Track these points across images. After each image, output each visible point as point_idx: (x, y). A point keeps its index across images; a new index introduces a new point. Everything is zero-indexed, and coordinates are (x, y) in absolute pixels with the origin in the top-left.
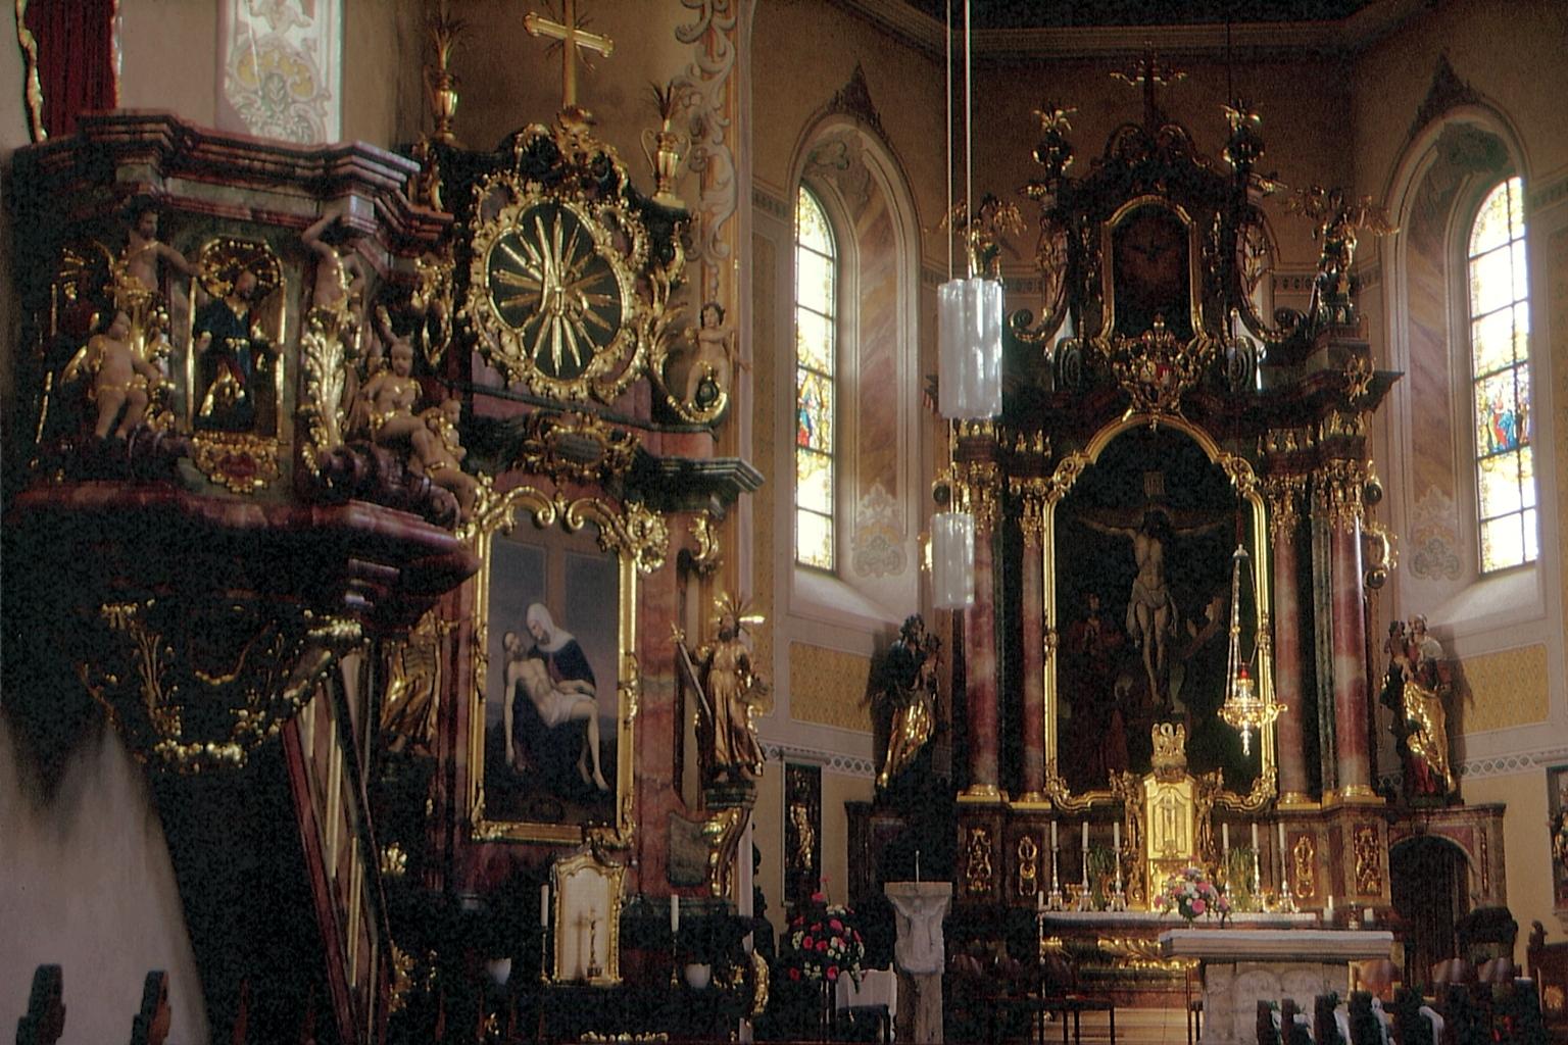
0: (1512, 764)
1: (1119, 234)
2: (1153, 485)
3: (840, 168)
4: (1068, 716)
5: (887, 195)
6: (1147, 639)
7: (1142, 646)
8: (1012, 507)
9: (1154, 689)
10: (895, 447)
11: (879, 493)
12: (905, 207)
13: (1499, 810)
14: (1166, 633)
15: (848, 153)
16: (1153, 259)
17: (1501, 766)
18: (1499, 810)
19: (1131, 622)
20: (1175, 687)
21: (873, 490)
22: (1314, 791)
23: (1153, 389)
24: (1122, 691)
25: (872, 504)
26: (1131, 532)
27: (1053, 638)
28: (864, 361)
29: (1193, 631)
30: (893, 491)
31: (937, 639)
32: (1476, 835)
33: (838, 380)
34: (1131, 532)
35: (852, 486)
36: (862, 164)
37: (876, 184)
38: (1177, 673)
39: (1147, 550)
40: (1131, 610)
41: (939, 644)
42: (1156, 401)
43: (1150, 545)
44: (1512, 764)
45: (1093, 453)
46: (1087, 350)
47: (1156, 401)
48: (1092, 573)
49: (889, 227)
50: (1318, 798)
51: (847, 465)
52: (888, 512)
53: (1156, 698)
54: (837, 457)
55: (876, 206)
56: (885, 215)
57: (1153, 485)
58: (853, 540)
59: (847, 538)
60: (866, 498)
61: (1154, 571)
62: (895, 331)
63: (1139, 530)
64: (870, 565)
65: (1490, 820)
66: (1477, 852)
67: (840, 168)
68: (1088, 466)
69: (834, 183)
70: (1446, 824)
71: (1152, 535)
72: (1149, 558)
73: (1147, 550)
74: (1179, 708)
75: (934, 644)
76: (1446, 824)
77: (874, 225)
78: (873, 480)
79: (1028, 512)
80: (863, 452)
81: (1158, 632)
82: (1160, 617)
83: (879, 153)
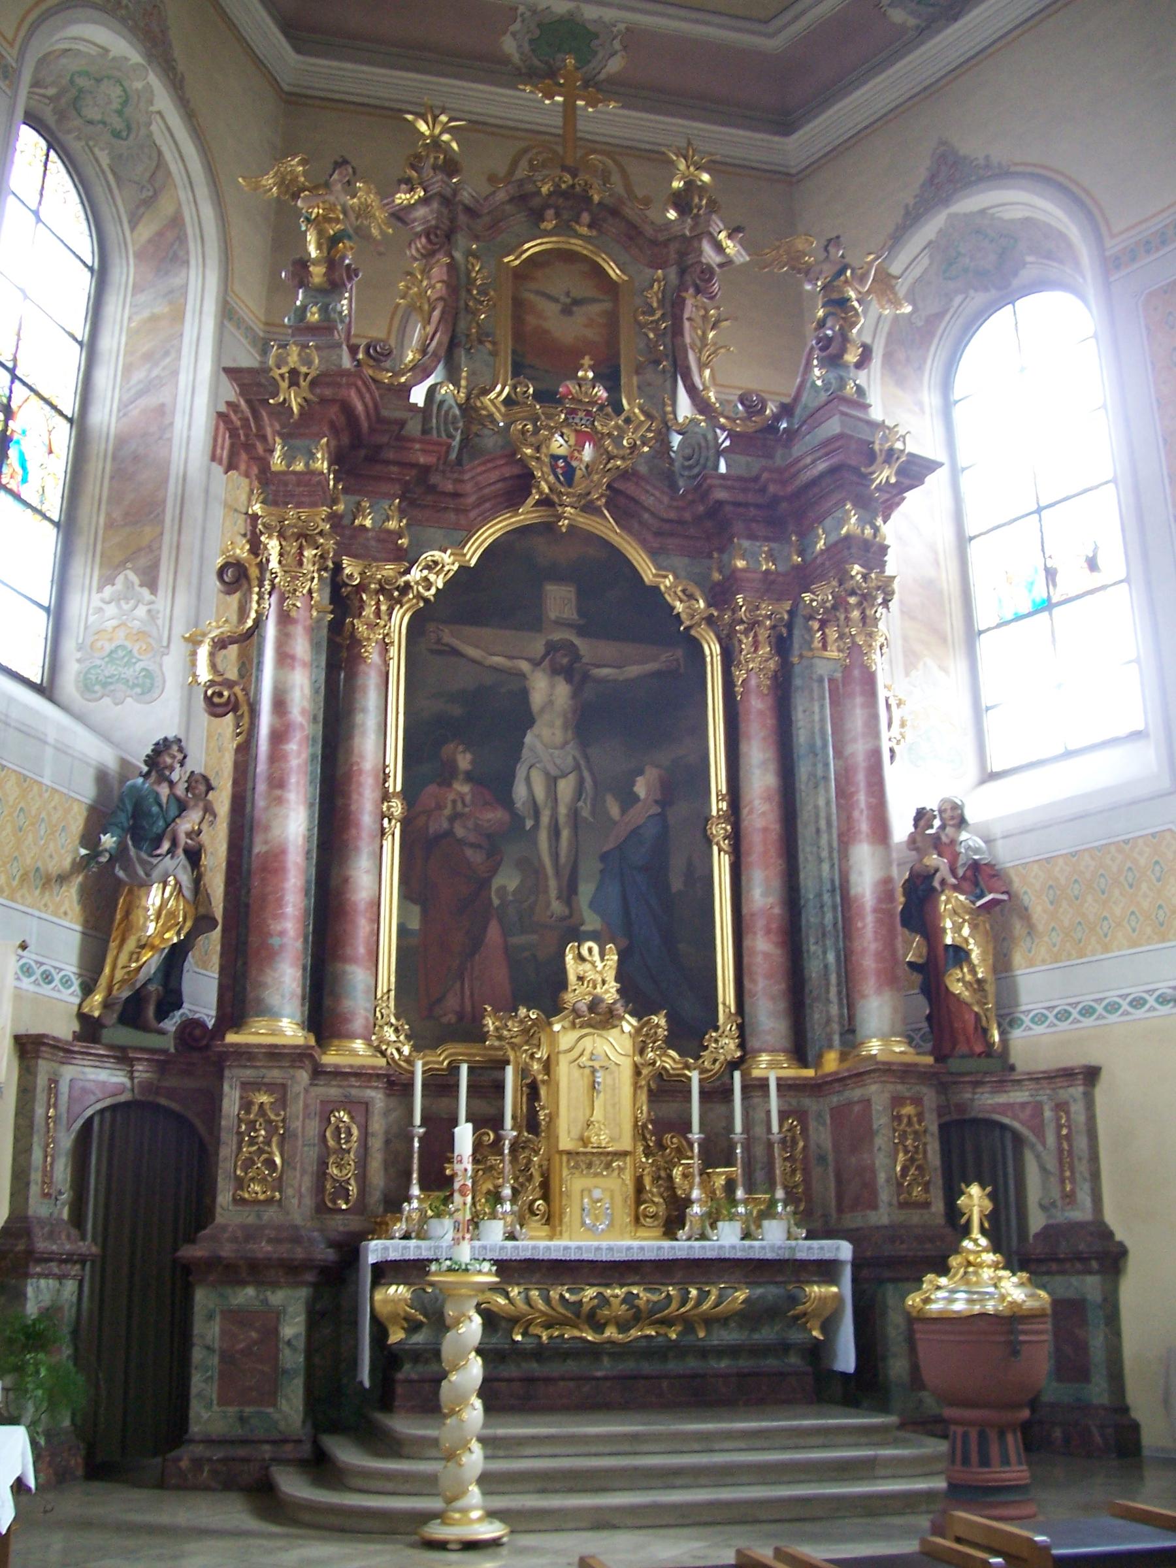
0: (1112, 1008)
1: (521, 275)
2: (559, 600)
3: (117, 135)
4: (415, 924)
5: (183, 195)
6: (545, 819)
7: (536, 826)
8: (343, 601)
9: (553, 893)
10: (162, 522)
11: (129, 585)
12: (208, 212)
13: (1091, 1074)
14: (574, 814)
15: (128, 110)
16: (567, 311)
17: (1088, 1011)
18: (1091, 1074)
19: (520, 792)
20: (586, 890)
21: (120, 580)
22: (800, 1052)
23: (568, 464)
24: (502, 890)
25: (116, 599)
26: (524, 666)
27: (397, 807)
28: (124, 406)
29: (614, 810)
30: (151, 584)
31: (206, 779)
32: (1048, 1114)
33: (79, 423)
34: (524, 666)
35: (83, 571)
36: (150, 135)
37: (169, 174)
38: (590, 868)
39: (548, 693)
40: (521, 772)
41: (210, 788)
42: (570, 485)
43: (552, 686)
44: (1112, 1008)
45: (473, 554)
46: (468, 409)
47: (570, 485)
48: (461, 728)
49: (182, 239)
50: (803, 1062)
51: (81, 543)
52: (141, 611)
53: (557, 907)
54: (68, 526)
55: (166, 207)
56: (176, 221)
57: (559, 600)
58: (80, 648)
59: (69, 647)
60: (108, 590)
61: (559, 722)
62: (175, 373)
63: (536, 664)
64: (105, 685)
65: (1078, 1091)
66: (1051, 1139)
67: (117, 135)
68: (463, 569)
69: (105, 161)
70: (1002, 1099)
71: (555, 671)
72: (551, 703)
73: (548, 693)
74: (592, 921)
75: (202, 788)
76: (1002, 1099)
77: (160, 234)
78: (122, 565)
79: (369, 612)
80: (110, 525)
81: (563, 810)
82: (566, 788)
83: (175, 120)
